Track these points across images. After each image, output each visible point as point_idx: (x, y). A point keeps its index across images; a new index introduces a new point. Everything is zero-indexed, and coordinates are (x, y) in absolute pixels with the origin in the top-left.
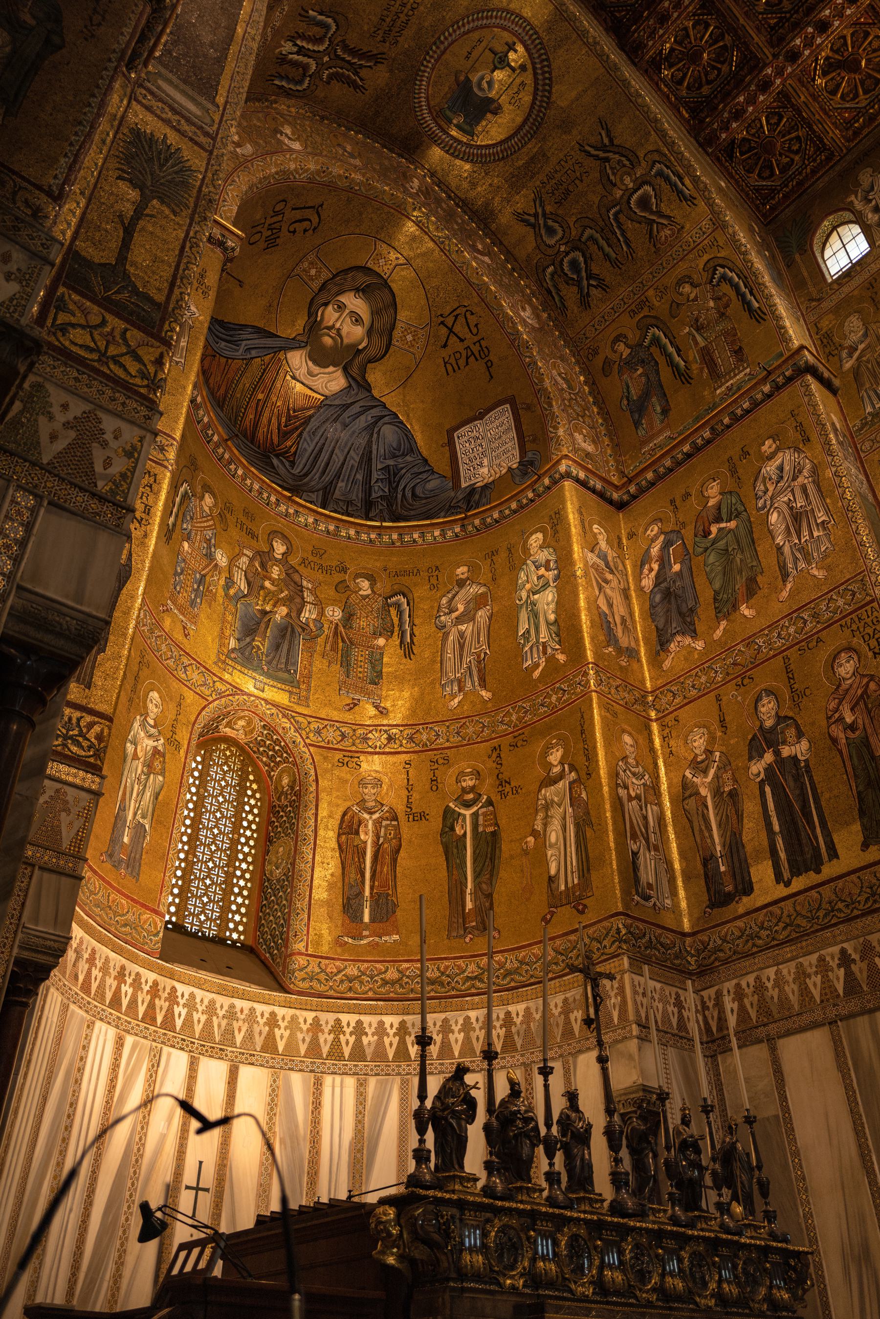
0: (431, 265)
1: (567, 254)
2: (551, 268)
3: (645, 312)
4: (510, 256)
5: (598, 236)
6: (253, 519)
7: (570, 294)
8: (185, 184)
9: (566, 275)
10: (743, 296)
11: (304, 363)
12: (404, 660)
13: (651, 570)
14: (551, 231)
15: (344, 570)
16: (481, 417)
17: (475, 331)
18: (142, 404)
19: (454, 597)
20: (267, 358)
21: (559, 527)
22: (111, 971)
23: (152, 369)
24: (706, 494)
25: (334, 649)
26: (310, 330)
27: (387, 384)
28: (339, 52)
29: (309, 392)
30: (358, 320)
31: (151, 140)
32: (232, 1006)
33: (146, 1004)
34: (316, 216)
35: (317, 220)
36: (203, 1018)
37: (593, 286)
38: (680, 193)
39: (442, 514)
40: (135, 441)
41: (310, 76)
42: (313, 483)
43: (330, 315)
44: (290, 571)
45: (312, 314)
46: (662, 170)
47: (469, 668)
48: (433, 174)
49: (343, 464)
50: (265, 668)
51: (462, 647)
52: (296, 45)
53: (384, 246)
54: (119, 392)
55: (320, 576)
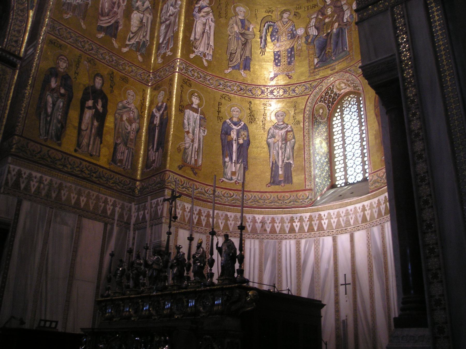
22: (286, 221)
32: (347, 210)
33: (308, 226)
36: (336, 220)
50: (334, 58)
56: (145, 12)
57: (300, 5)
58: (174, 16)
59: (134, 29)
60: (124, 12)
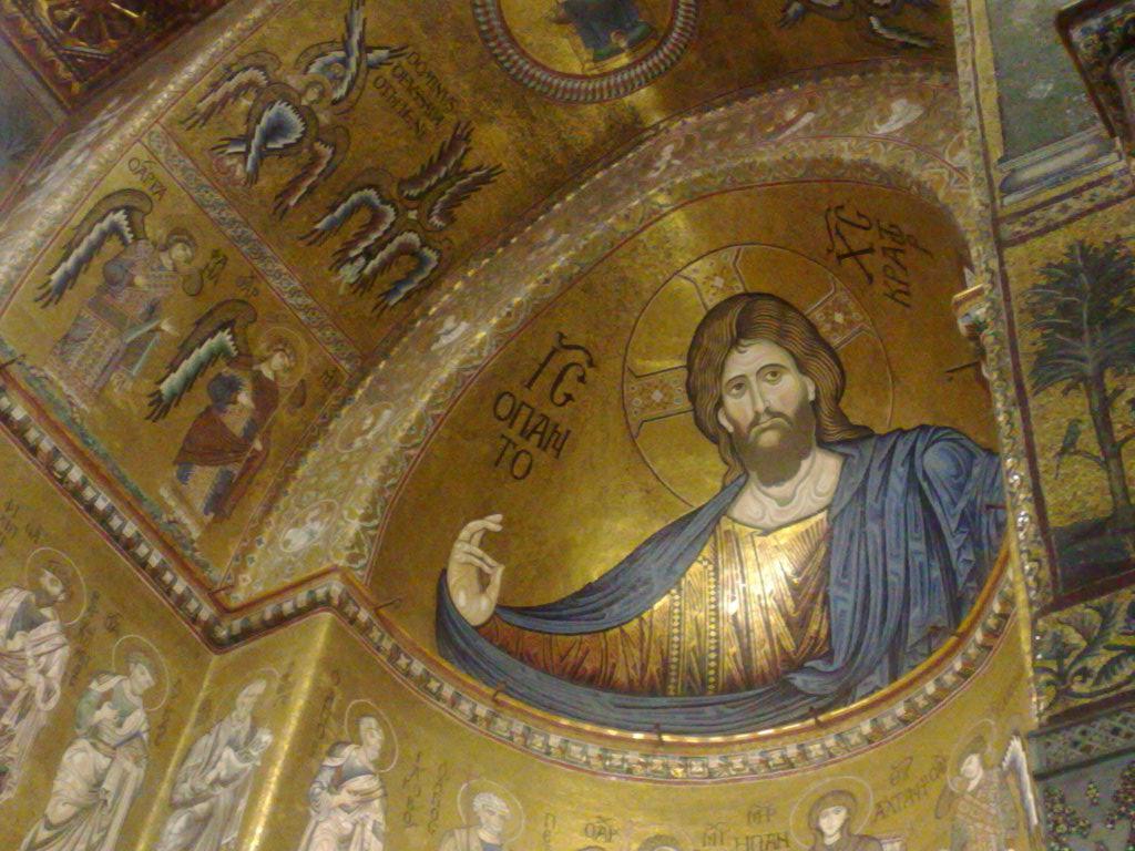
2: (875, 22)
4: (841, 67)
11: (767, 500)
17: (864, 222)
20: (707, 552)
28: (414, 192)
29: (800, 527)
30: (774, 371)
41: (423, 246)
52: (357, 257)
56: (123, 749)
57: (720, 826)
58: (231, 787)
59: (59, 810)
60: (37, 740)
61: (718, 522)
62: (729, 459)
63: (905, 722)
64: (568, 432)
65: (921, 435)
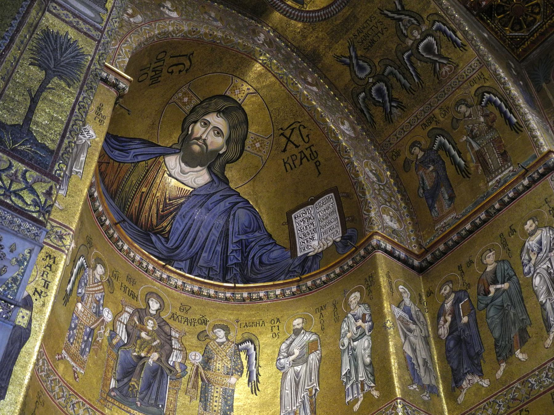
0: (274, 93)
1: (374, 84)
2: (363, 94)
3: (433, 125)
4: (332, 86)
5: (396, 71)
6: (134, 283)
7: (378, 113)
8: (78, 65)
9: (374, 99)
10: (505, 114)
11: (178, 164)
12: (251, 396)
13: (446, 321)
14: (362, 69)
15: (205, 322)
16: (312, 202)
18: (33, 225)
19: (291, 344)
20: (150, 162)
21: (372, 288)
23: (43, 199)
24: (485, 262)
25: (195, 386)
26: (183, 141)
27: (241, 179)
30: (219, 133)
31: (57, 36)
34: (188, 62)
35: (189, 64)
37: (394, 106)
38: (454, 42)
39: (283, 277)
40: (26, 252)
42: (182, 254)
43: (198, 130)
44: (162, 324)
45: (184, 129)
46: (440, 26)
47: (303, 402)
48: (275, 30)
49: (206, 239)
50: (139, 404)
51: (297, 384)
53: (239, 80)
54: (17, 217)
55: (185, 327)
61: (160, 156)
62: (180, 141)
63: (193, 292)
64: (159, 82)
65: (244, 202)
